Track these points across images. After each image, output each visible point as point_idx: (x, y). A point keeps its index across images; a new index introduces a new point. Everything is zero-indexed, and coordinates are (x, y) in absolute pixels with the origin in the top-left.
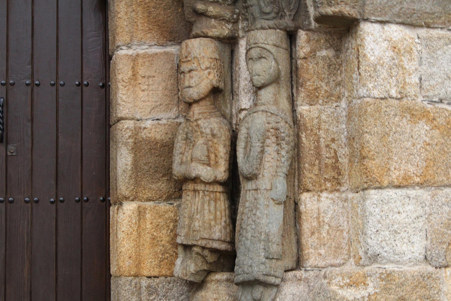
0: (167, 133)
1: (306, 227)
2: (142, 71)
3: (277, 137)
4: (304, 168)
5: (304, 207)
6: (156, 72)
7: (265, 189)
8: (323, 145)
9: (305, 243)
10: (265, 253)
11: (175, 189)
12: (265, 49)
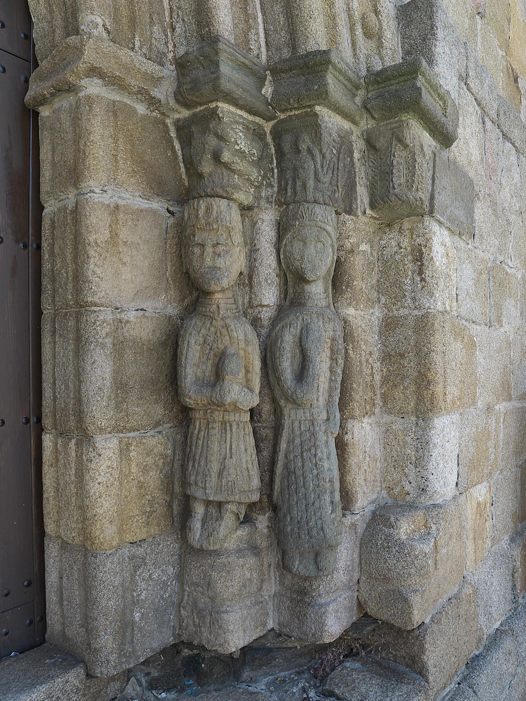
0: (154, 331)
1: (353, 461)
2: (124, 234)
3: (332, 350)
4: (352, 388)
5: (350, 437)
6: (140, 238)
7: (322, 419)
8: (363, 359)
9: (351, 482)
10: (332, 507)
11: (165, 411)
12: (324, 229)
